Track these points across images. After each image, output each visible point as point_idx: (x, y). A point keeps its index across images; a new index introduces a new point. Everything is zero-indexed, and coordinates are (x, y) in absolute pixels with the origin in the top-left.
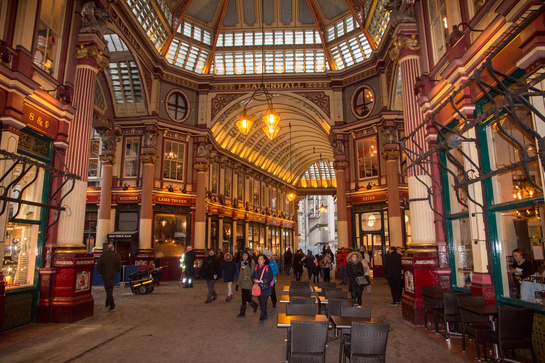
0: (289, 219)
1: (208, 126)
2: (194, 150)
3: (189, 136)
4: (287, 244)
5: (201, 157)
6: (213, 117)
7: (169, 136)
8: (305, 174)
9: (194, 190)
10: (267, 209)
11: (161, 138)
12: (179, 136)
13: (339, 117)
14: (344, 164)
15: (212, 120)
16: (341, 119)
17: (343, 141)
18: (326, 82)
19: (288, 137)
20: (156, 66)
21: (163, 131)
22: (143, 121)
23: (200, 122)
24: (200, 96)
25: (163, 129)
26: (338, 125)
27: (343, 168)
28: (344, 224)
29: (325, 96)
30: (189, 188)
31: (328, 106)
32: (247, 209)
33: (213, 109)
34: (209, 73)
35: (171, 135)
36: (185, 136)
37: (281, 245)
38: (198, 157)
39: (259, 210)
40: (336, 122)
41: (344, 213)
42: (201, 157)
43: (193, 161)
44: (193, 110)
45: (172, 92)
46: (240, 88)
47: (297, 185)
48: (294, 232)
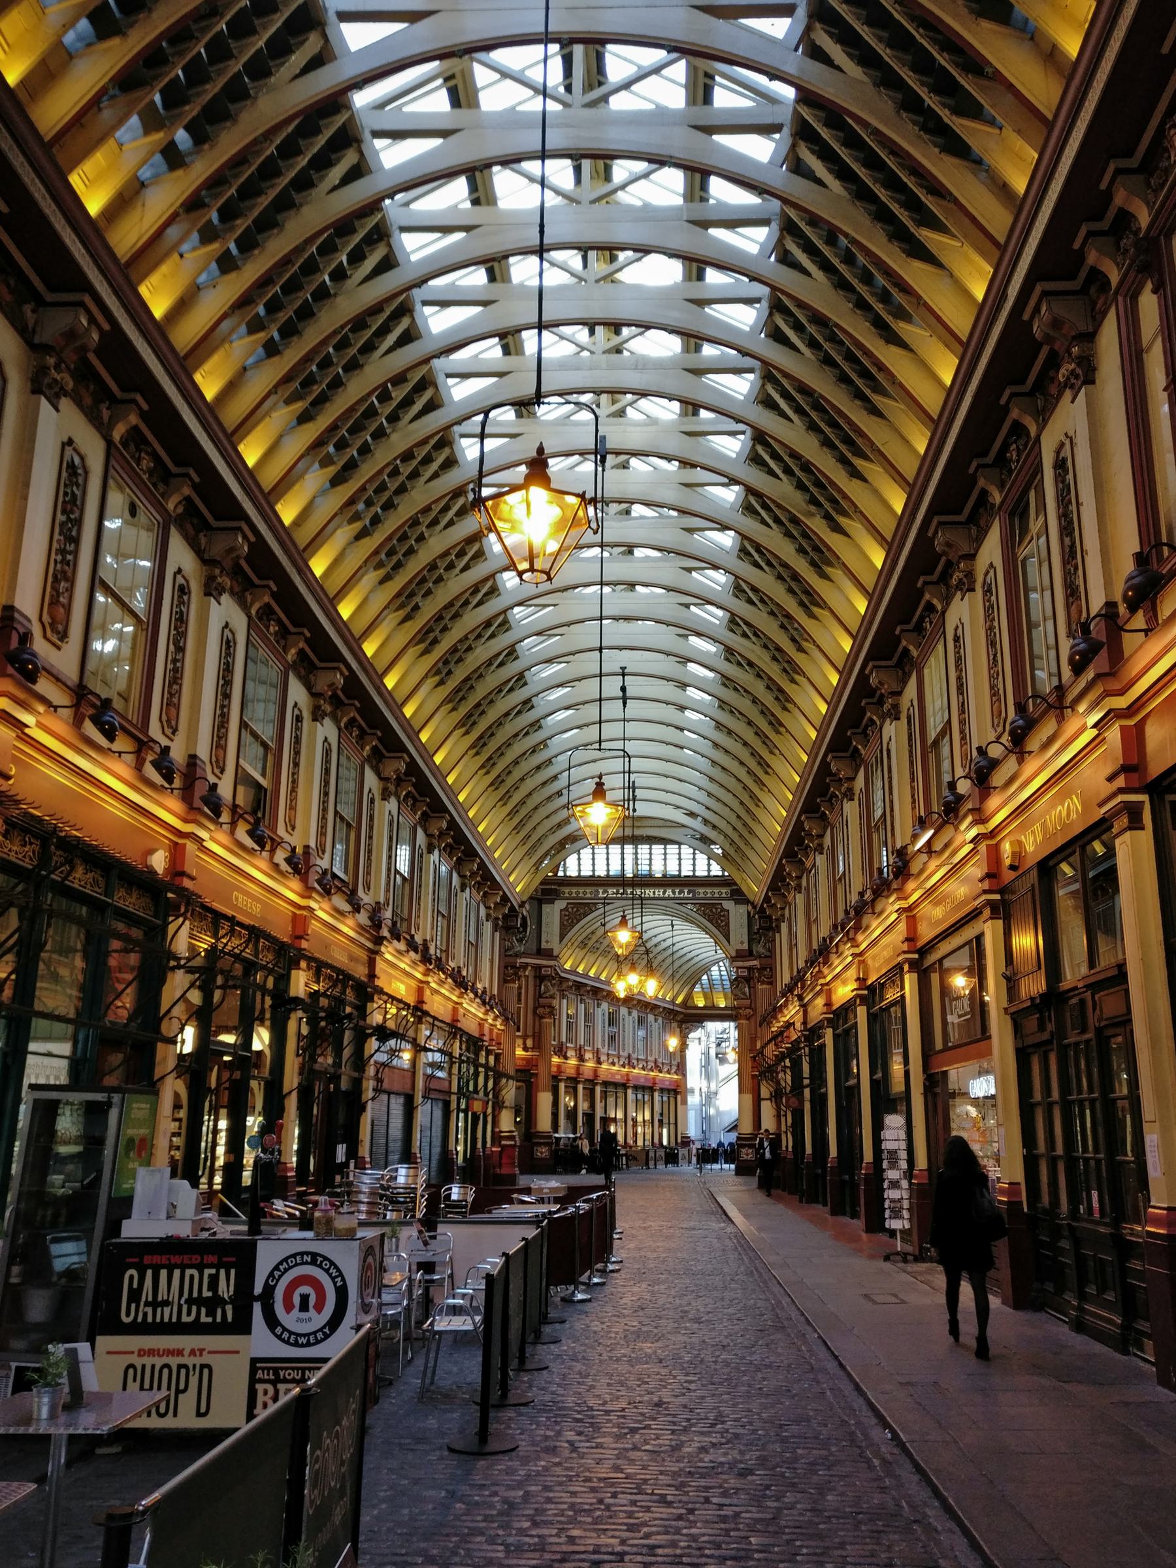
0: (669, 1072)
1: (555, 953)
2: (535, 986)
4: (665, 1120)
6: (562, 938)
8: (700, 979)
9: (537, 1046)
10: (629, 1057)
13: (742, 943)
15: (561, 941)
17: (748, 980)
18: (724, 890)
19: (669, 942)
23: (544, 945)
26: (739, 956)
27: (748, 1019)
28: (749, 1098)
29: (723, 910)
30: (529, 1043)
31: (727, 924)
32: (599, 1062)
33: (562, 923)
34: (556, 874)
37: (652, 1123)
39: (616, 1060)
40: (737, 951)
41: (749, 1082)
46: (601, 895)
47: (684, 1003)
48: (679, 1097)
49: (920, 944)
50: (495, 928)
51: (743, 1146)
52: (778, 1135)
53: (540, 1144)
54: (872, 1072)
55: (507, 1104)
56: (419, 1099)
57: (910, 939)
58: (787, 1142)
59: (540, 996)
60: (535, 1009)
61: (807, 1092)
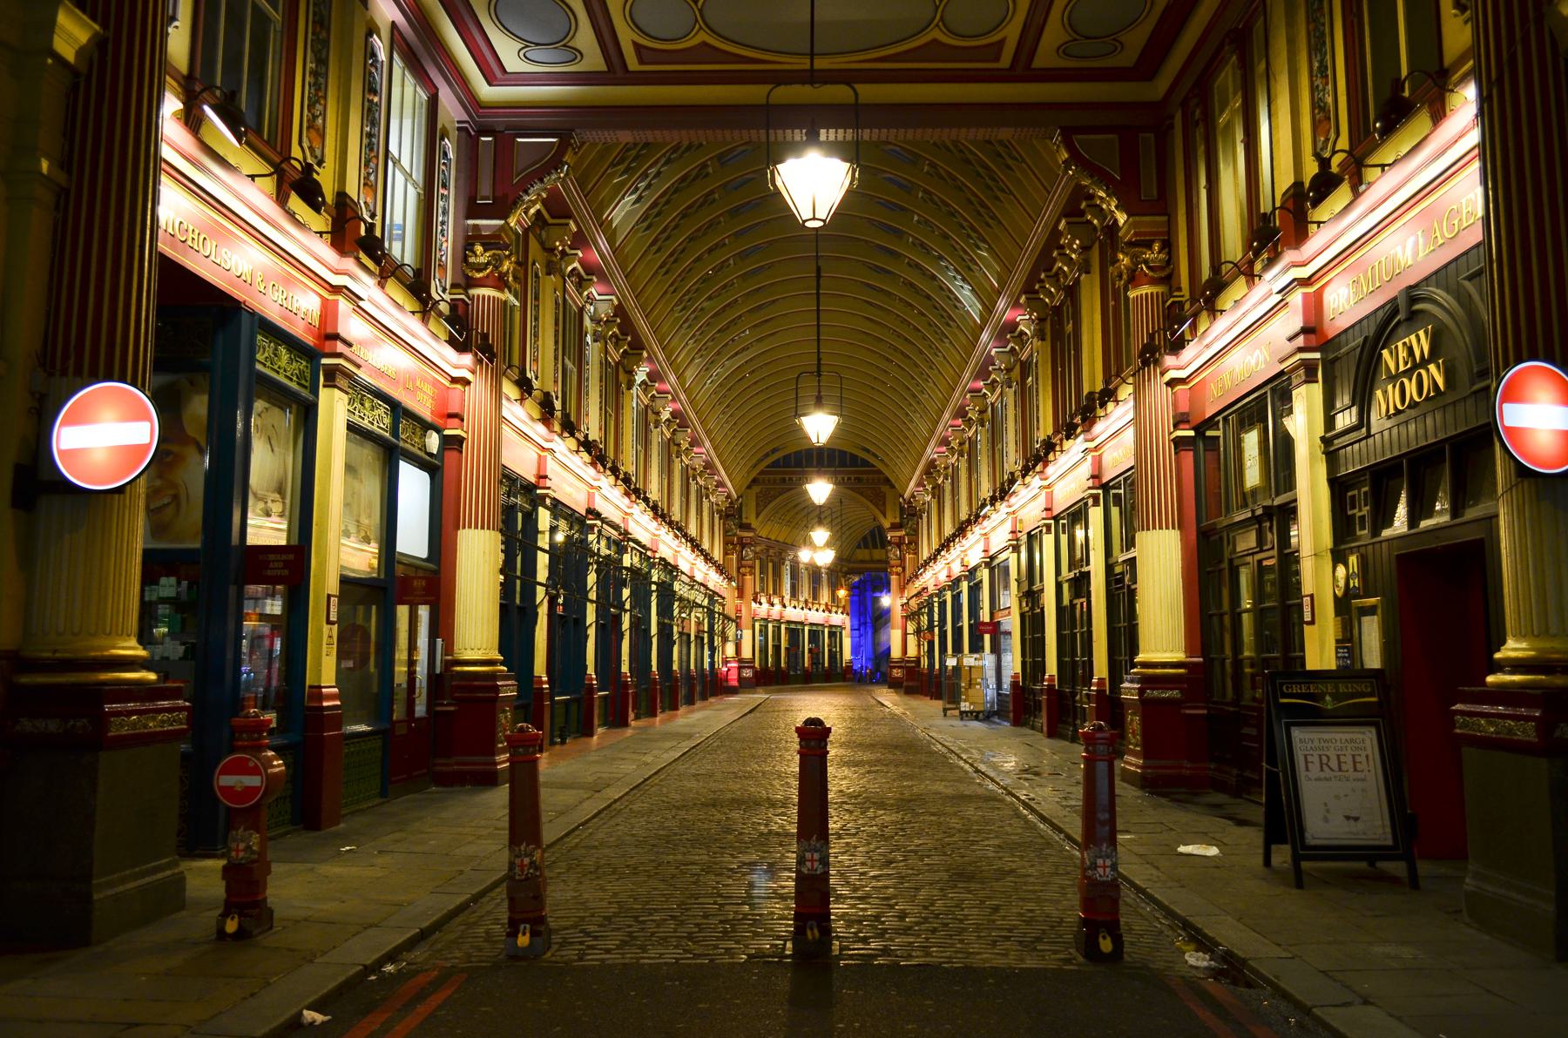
1: (753, 526)
14: (900, 569)
16: (898, 520)
23: (744, 521)
27: (898, 574)
32: (784, 606)
49: (991, 553)
50: (720, 519)
51: (895, 667)
52: (918, 659)
53: (745, 667)
54: (970, 620)
55: (730, 639)
56: (693, 638)
57: (985, 551)
58: (925, 662)
59: (742, 559)
60: (738, 569)
61: (936, 629)
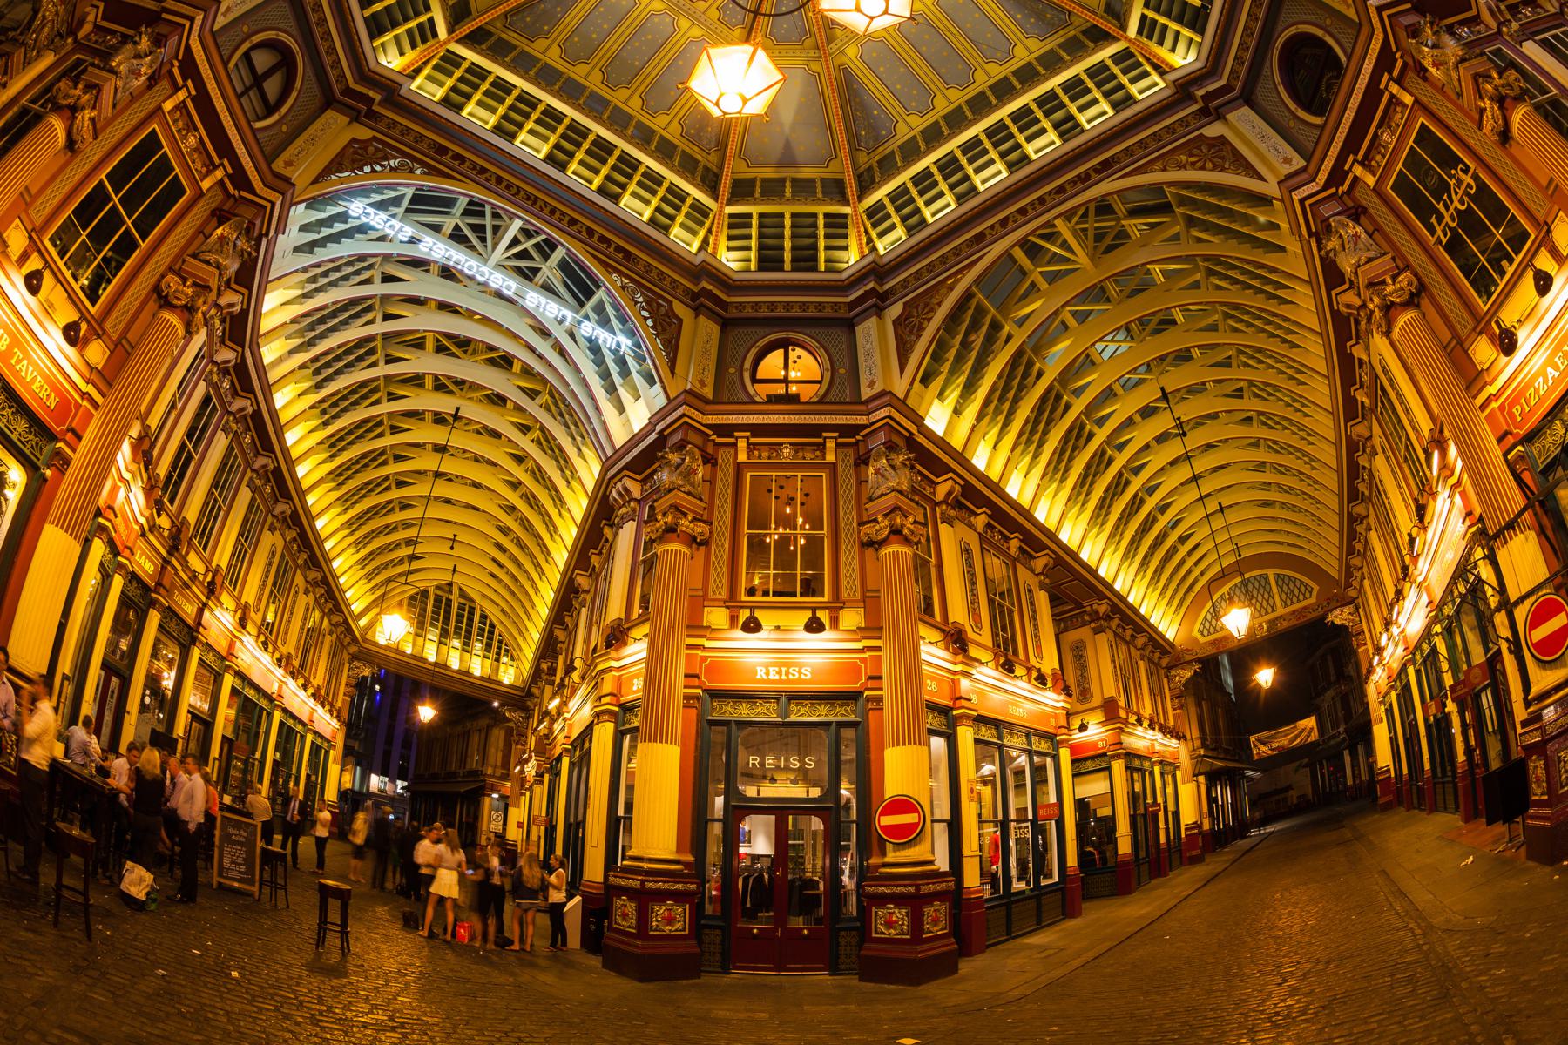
3: (831, 444)
5: (882, 495)
7: (760, 457)
11: (731, 470)
12: (796, 452)
20: (696, 289)
21: (735, 445)
22: (659, 428)
23: (866, 393)
24: (859, 329)
25: (731, 440)
30: (852, 618)
35: (765, 454)
36: (821, 448)
38: (871, 499)
42: (882, 495)
43: (859, 515)
44: (842, 371)
45: (761, 343)
53: (883, 900)
